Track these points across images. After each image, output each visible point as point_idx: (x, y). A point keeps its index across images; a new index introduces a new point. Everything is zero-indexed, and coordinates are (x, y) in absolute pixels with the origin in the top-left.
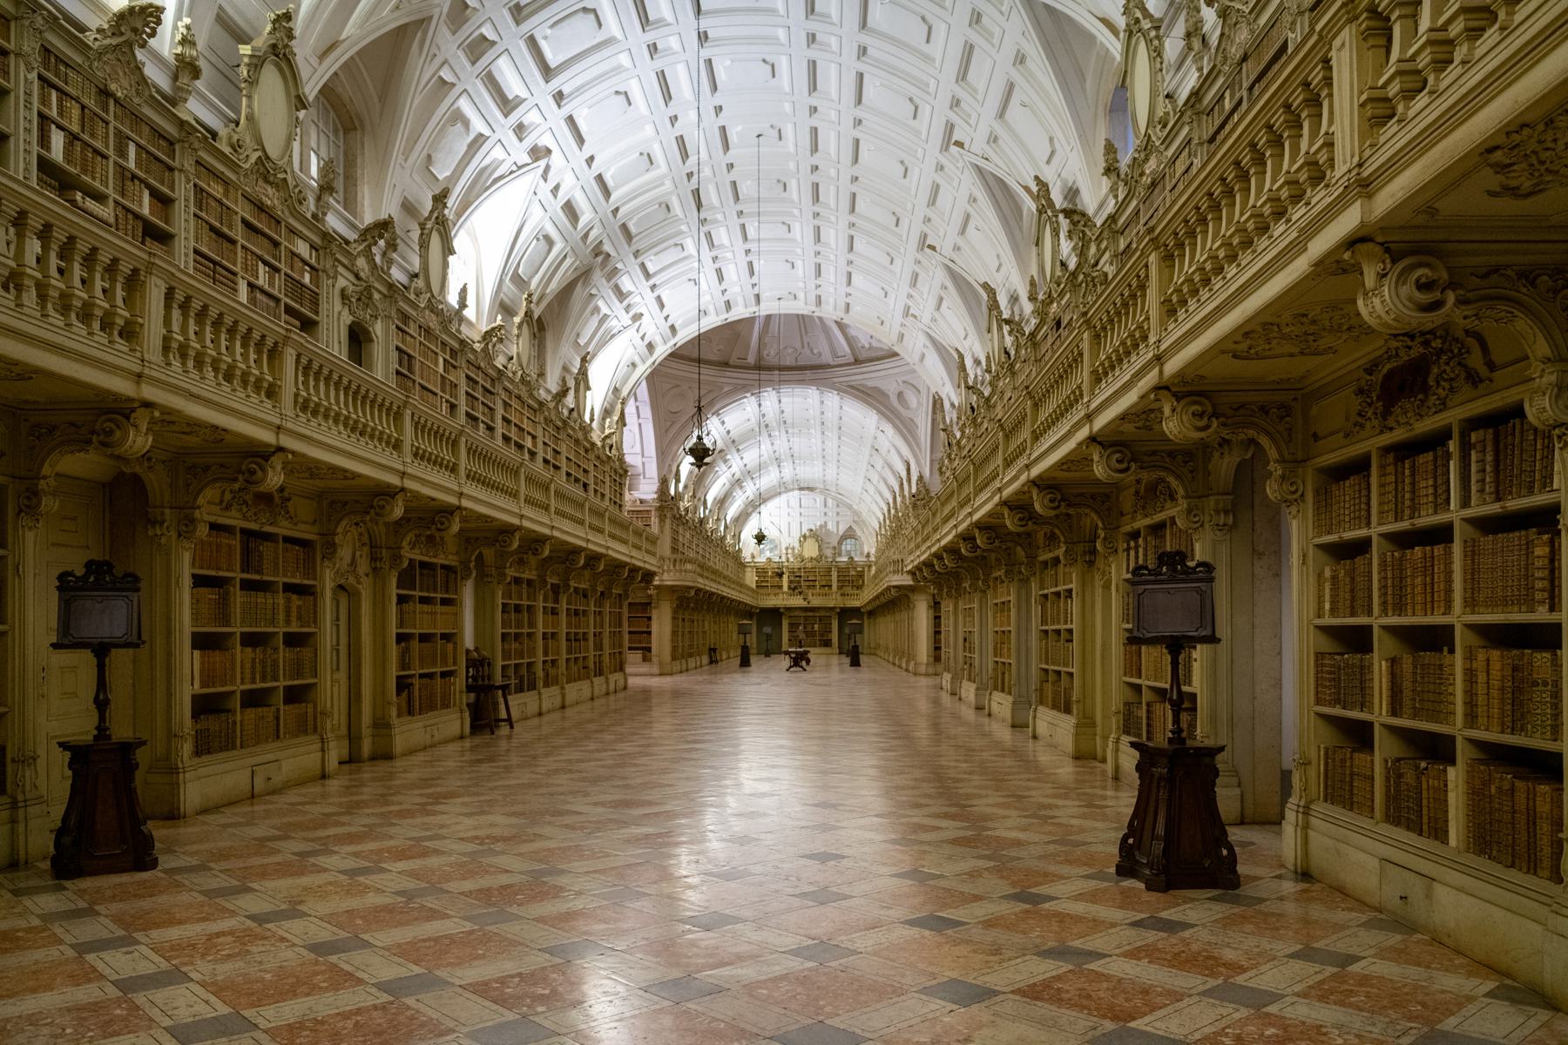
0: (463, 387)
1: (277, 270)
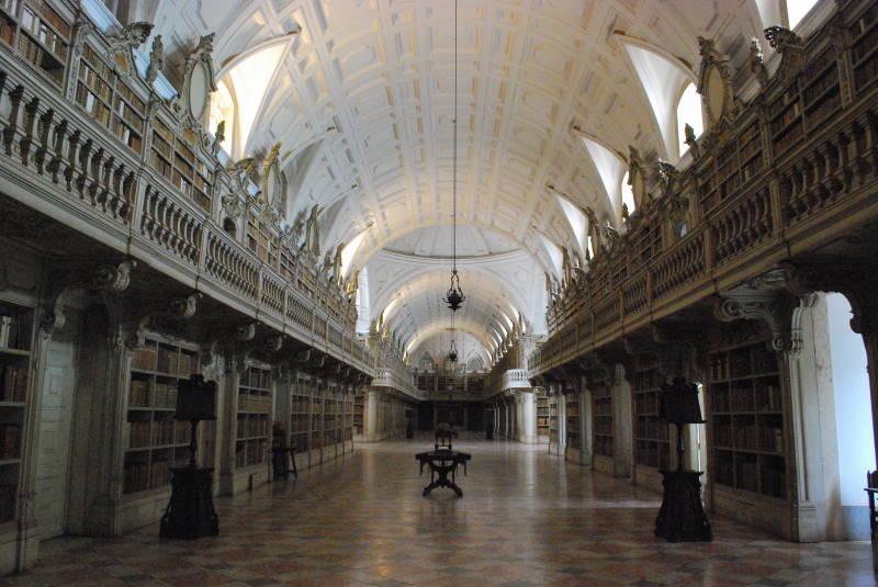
0: (280, 261)
1: (189, 183)
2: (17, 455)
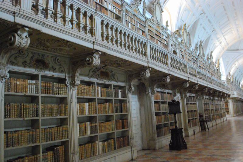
0: (192, 61)
1: (161, 42)
2: (128, 128)
